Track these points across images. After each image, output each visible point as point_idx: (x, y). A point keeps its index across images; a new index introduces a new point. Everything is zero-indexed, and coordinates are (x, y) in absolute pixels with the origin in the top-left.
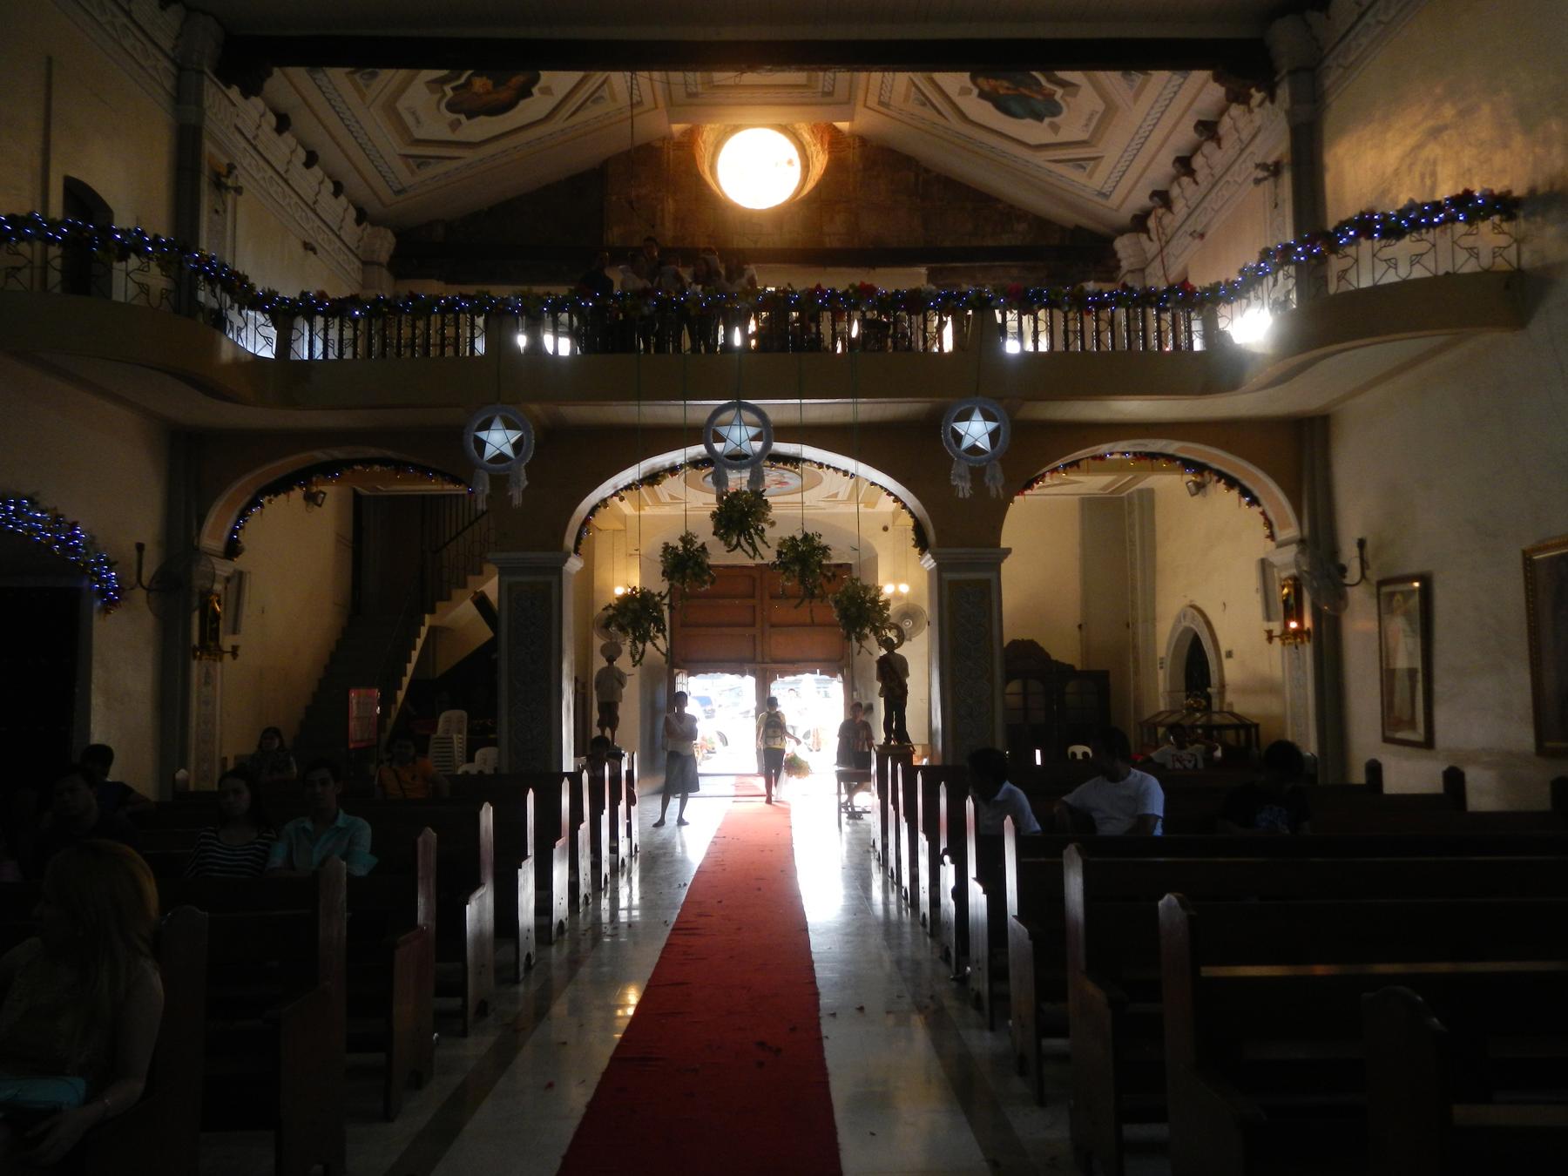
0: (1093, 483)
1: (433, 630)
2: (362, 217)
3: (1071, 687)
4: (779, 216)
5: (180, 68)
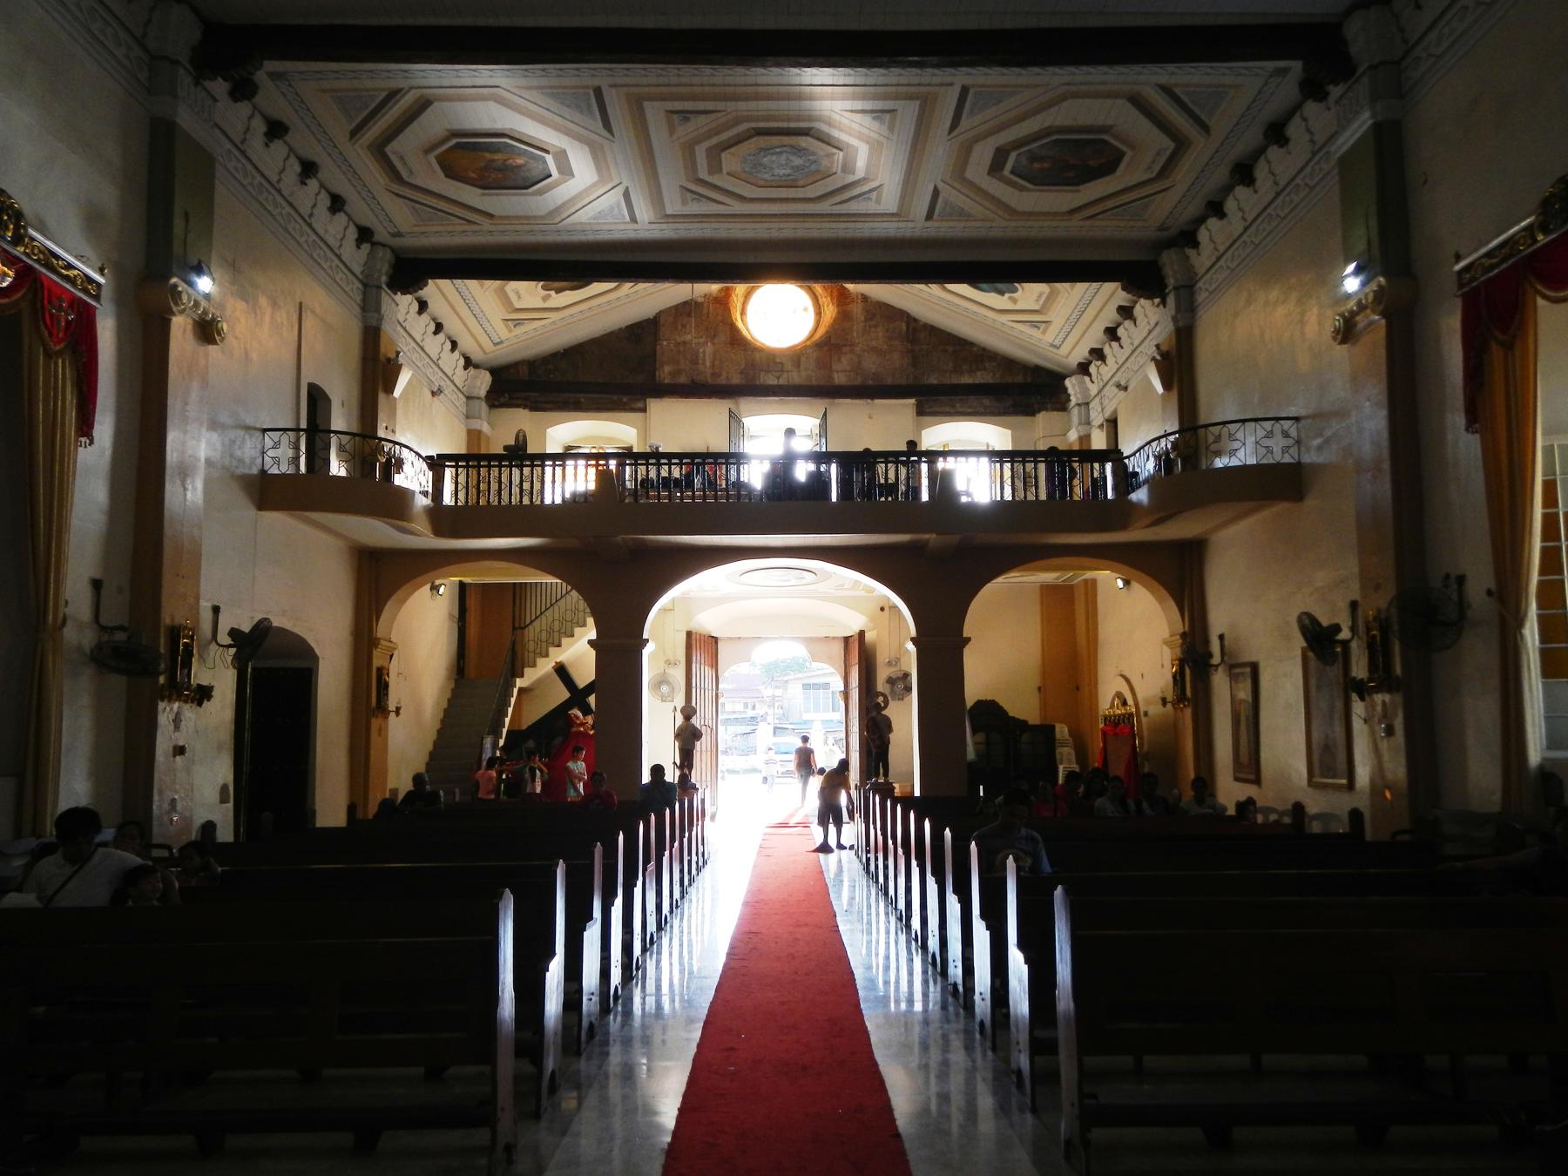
0: (1049, 577)
1: (521, 690)
2: (468, 363)
3: (1025, 738)
4: (797, 355)
5: (365, 285)
